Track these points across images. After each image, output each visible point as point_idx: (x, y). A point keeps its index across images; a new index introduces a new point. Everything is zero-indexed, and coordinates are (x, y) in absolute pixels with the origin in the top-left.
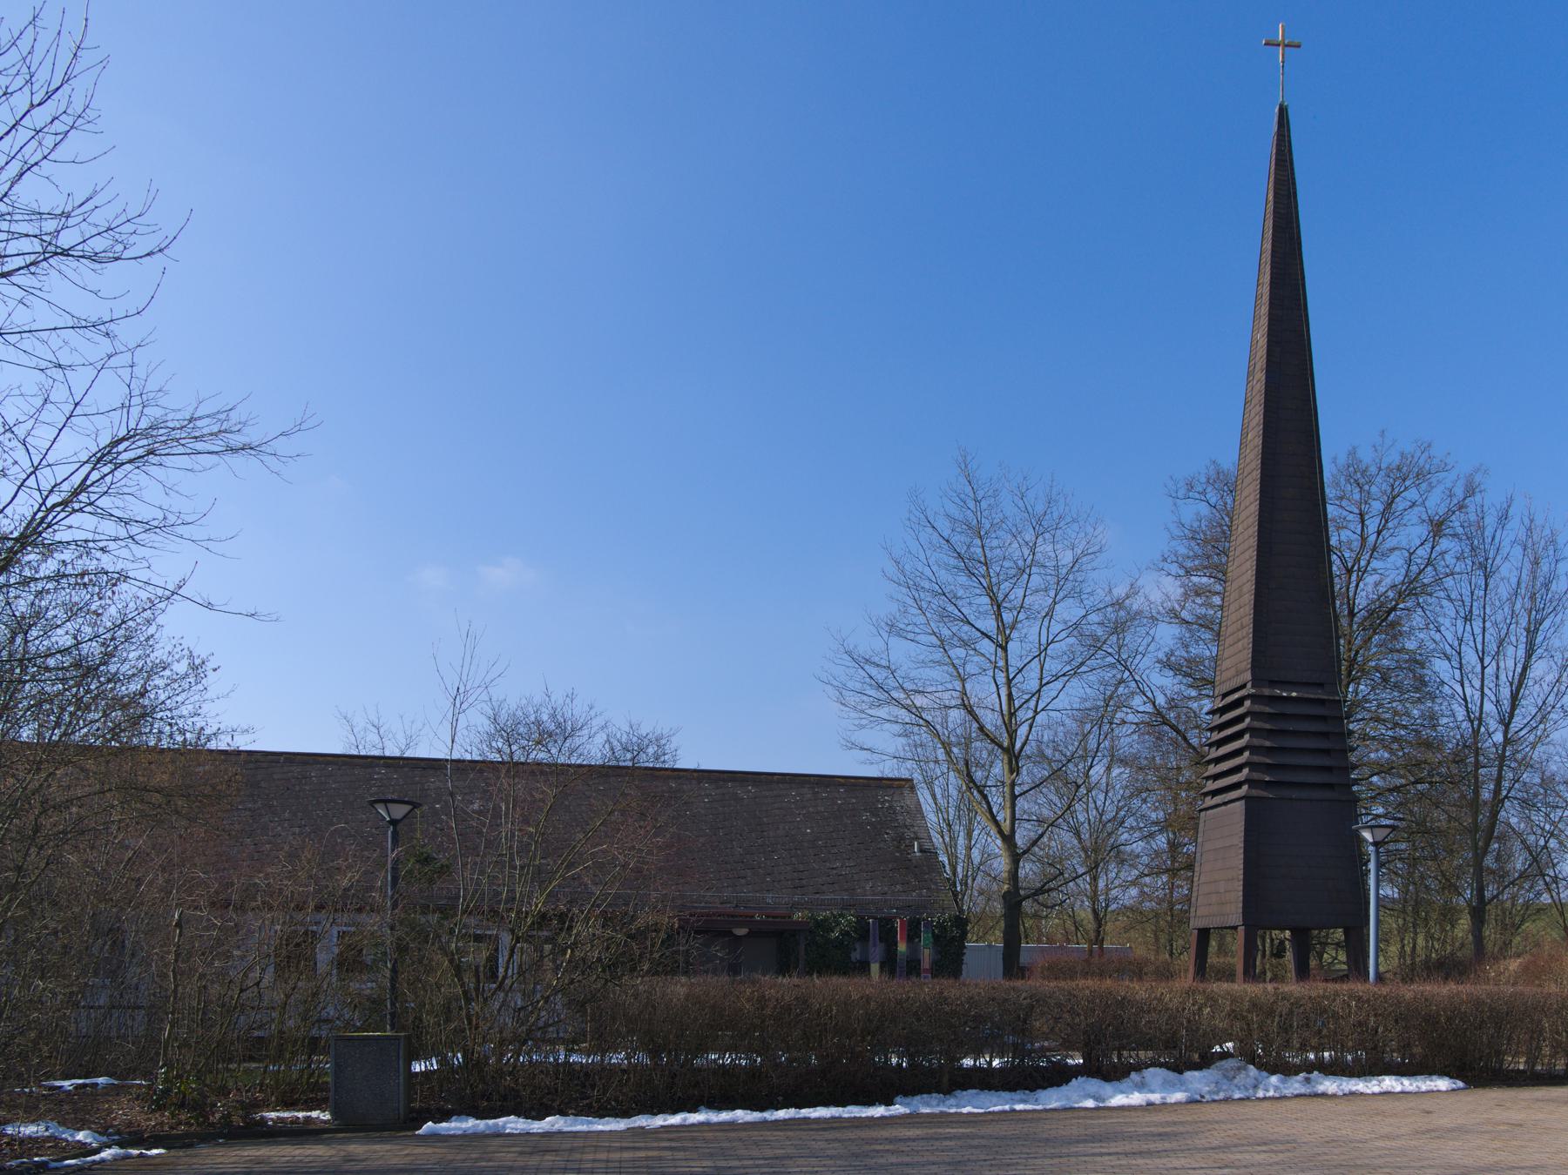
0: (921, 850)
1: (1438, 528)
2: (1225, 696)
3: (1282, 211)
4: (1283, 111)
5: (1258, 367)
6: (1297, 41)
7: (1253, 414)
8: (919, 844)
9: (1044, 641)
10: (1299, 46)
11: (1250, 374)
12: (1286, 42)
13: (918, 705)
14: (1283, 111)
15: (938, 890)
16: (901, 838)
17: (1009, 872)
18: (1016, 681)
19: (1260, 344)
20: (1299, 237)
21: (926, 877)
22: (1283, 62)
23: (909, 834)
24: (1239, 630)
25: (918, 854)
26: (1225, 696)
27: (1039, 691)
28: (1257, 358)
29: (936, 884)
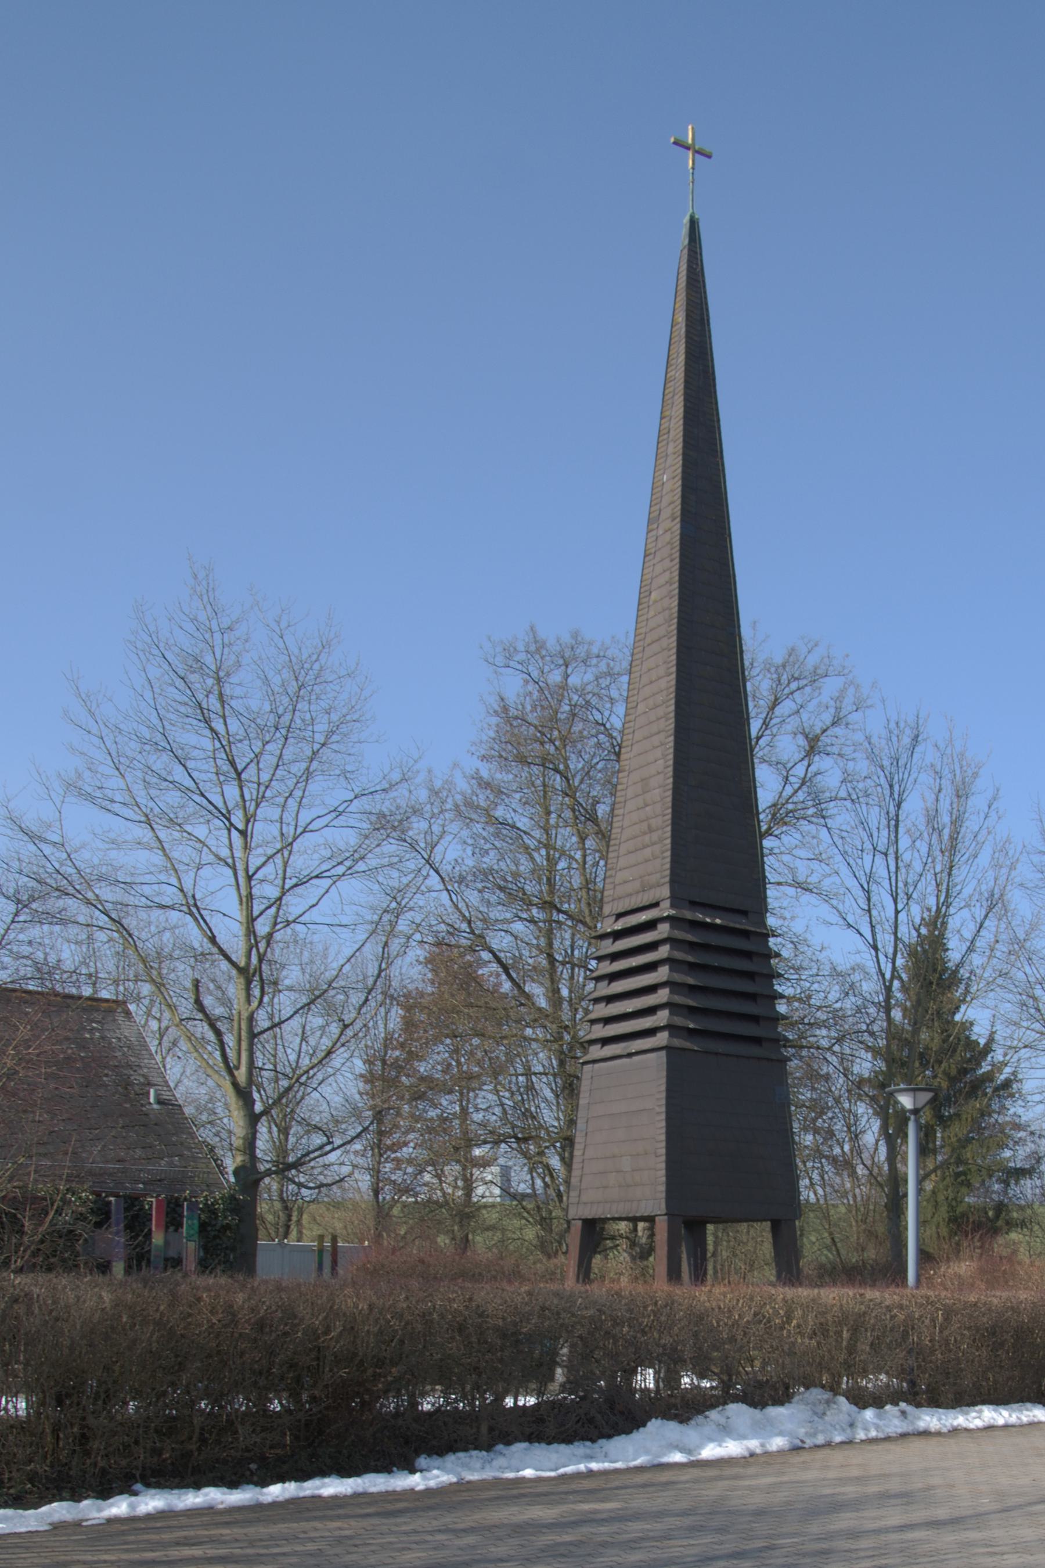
0: (159, 1102)
1: (813, 746)
2: (619, 916)
3: (696, 338)
4: (694, 224)
5: (666, 513)
6: (707, 149)
7: (659, 568)
8: (156, 1091)
9: (289, 831)
10: (709, 156)
11: (653, 521)
12: (697, 147)
13: (104, 897)
14: (694, 224)
15: (195, 1159)
16: (127, 1084)
17: (244, 1138)
18: (259, 875)
19: (668, 487)
20: (713, 373)
21: (174, 1139)
22: (693, 168)
23: (137, 1078)
24: (645, 833)
25: (156, 1106)
26: (619, 916)
27: (280, 899)
28: (664, 503)
29: (190, 1149)
